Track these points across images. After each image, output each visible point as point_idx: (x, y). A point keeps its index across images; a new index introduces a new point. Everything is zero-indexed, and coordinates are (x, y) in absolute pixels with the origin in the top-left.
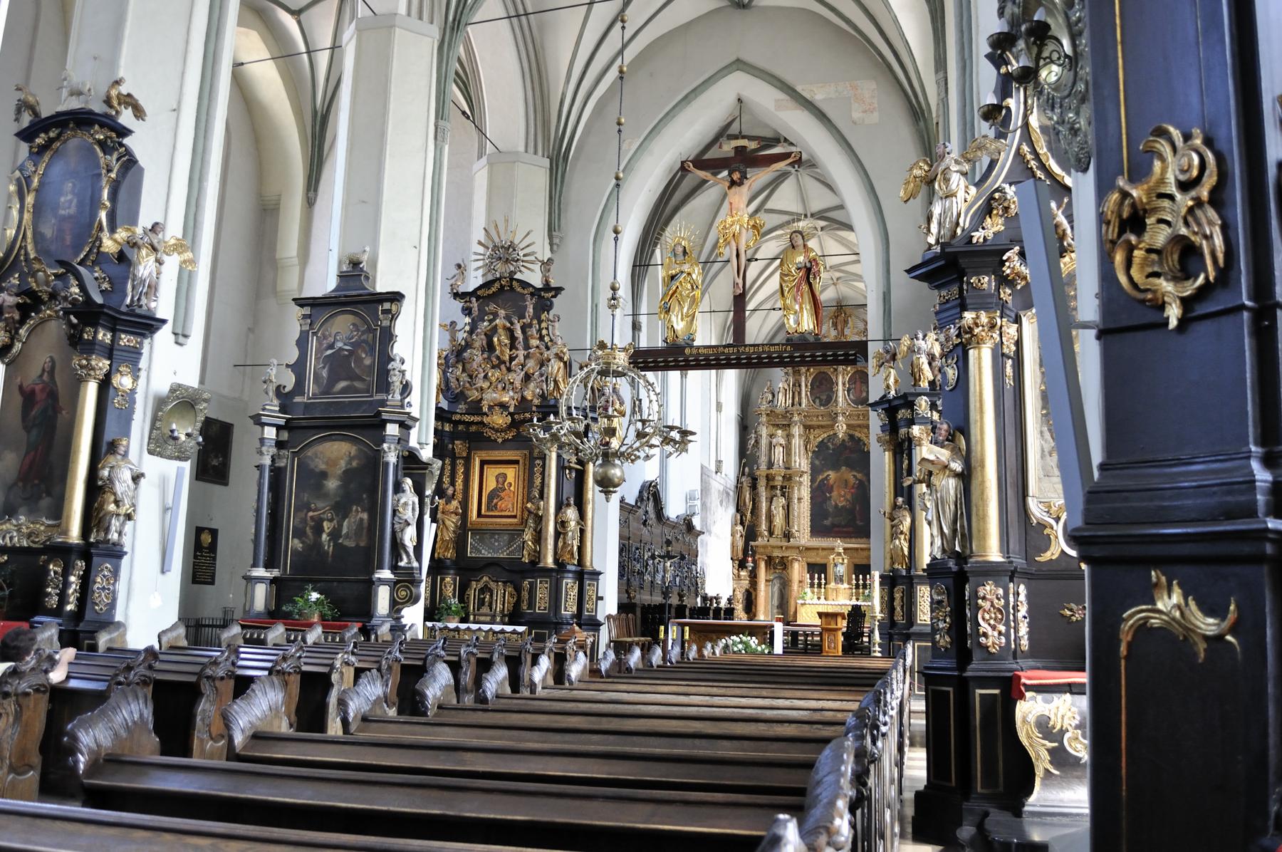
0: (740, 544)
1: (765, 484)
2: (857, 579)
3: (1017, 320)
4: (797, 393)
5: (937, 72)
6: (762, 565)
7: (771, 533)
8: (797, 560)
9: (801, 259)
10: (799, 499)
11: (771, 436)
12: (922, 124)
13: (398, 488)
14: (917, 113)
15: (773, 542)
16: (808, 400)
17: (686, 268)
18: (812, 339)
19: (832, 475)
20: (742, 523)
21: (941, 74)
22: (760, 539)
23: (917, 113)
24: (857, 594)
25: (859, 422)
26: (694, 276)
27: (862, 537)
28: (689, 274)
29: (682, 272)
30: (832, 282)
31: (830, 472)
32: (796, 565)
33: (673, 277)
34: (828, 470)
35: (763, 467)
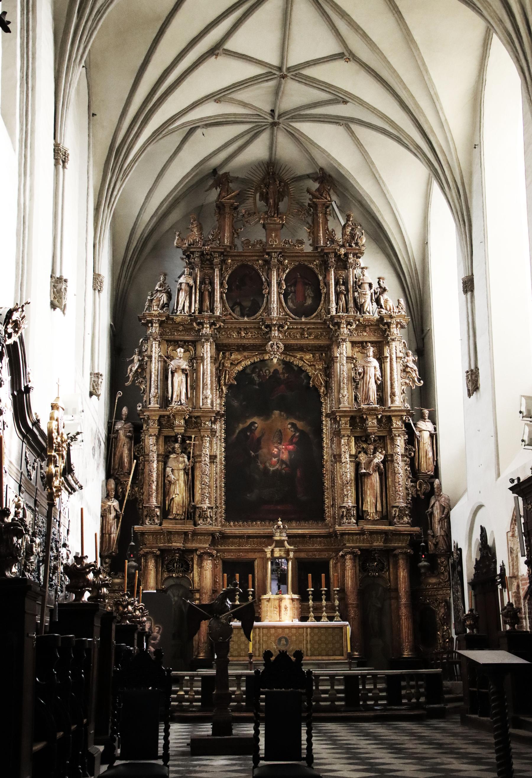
0: (115, 533)
1: (156, 431)
4: (207, 293)
6: (151, 565)
8: (211, 555)
10: (213, 458)
11: (166, 359)
15: (167, 525)
16: (224, 306)
19: (258, 422)
22: (147, 521)
25: (303, 342)
27: (306, 519)
30: (270, 120)
31: (255, 419)
32: (208, 564)
34: (253, 415)
35: (154, 405)
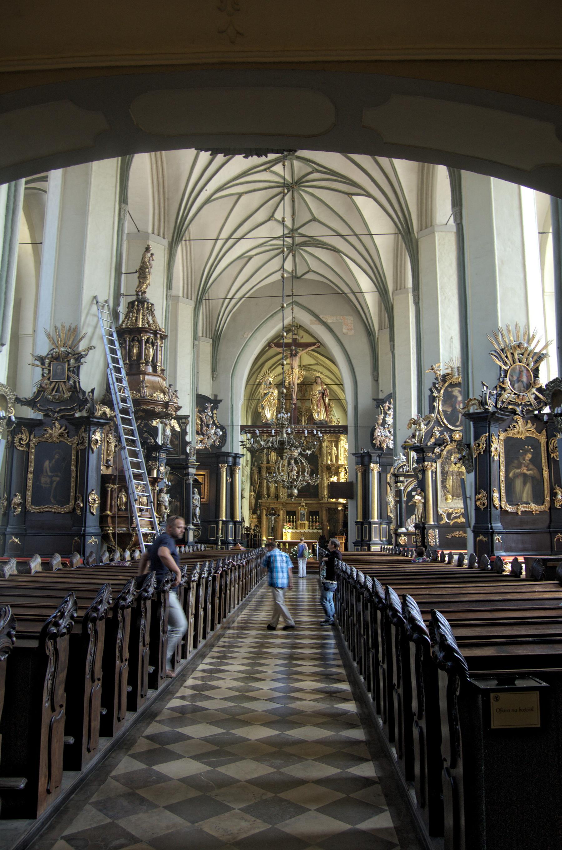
0: (253, 502)
2: (312, 519)
3: (436, 462)
5: (390, 341)
7: (269, 496)
9: (320, 388)
12: (372, 337)
13: (194, 493)
14: (369, 333)
17: (271, 390)
18: (324, 422)
20: (254, 491)
21: (392, 343)
23: (369, 333)
24: (312, 525)
26: (275, 394)
27: (313, 498)
28: (272, 393)
29: (269, 392)
33: (265, 394)
35: (265, 462)
